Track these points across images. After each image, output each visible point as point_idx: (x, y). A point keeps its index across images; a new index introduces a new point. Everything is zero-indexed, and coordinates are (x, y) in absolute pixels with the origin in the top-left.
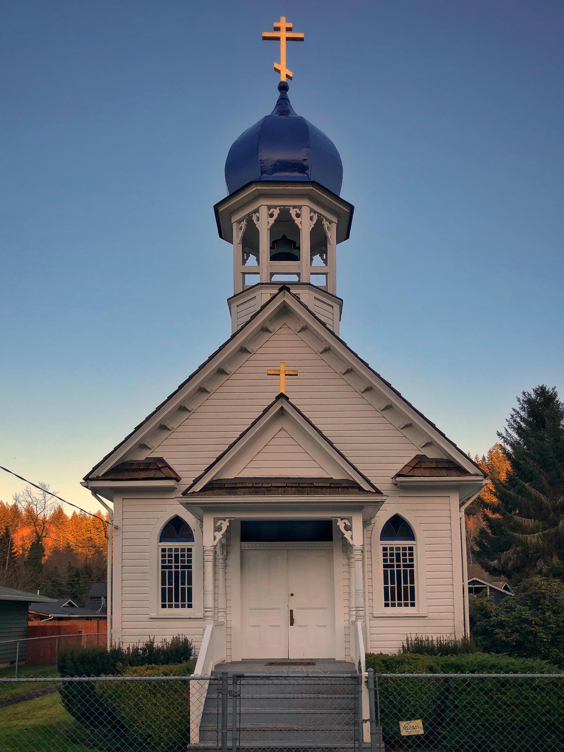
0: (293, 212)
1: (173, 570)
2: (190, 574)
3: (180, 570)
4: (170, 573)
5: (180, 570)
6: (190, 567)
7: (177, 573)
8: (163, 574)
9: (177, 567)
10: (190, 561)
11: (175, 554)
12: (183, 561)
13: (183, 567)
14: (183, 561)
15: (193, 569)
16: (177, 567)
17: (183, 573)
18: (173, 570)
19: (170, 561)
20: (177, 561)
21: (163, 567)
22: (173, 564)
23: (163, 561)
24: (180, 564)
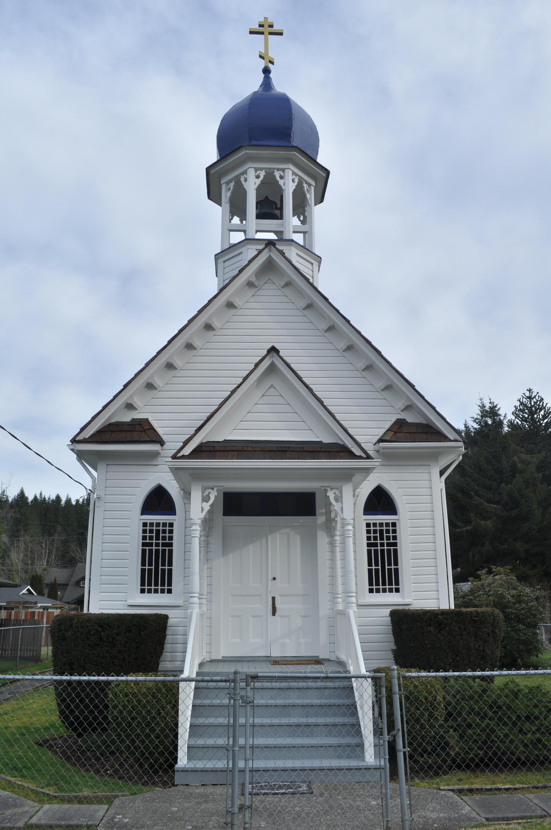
0: (277, 174)
1: (154, 548)
2: (171, 552)
3: (160, 548)
4: (150, 551)
5: (160, 548)
6: (171, 545)
7: (157, 551)
8: (144, 552)
9: (157, 545)
10: (171, 538)
11: (156, 530)
12: (164, 538)
13: (164, 545)
14: (164, 538)
15: (175, 548)
16: (157, 545)
17: (164, 551)
18: (154, 548)
19: (151, 538)
20: (157, 538)
21: (144, 545)
22: (154, 541)
23: (144, 538)
24: (161, 541)
